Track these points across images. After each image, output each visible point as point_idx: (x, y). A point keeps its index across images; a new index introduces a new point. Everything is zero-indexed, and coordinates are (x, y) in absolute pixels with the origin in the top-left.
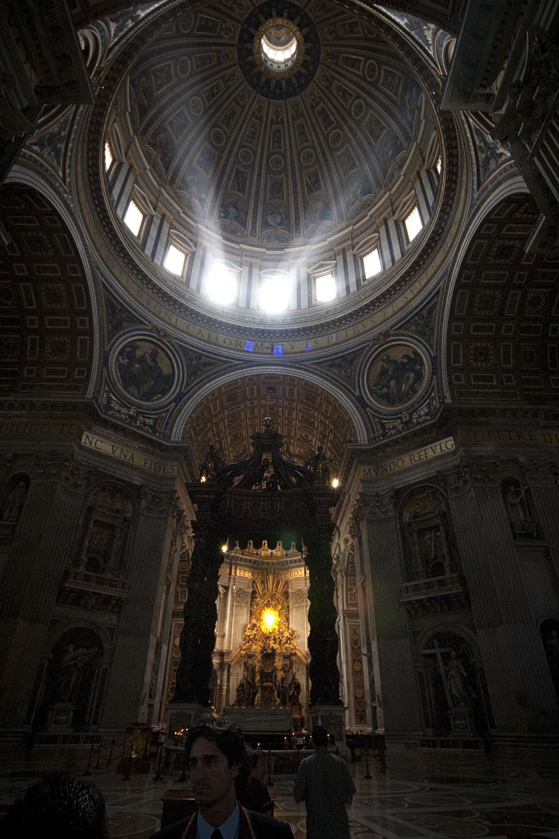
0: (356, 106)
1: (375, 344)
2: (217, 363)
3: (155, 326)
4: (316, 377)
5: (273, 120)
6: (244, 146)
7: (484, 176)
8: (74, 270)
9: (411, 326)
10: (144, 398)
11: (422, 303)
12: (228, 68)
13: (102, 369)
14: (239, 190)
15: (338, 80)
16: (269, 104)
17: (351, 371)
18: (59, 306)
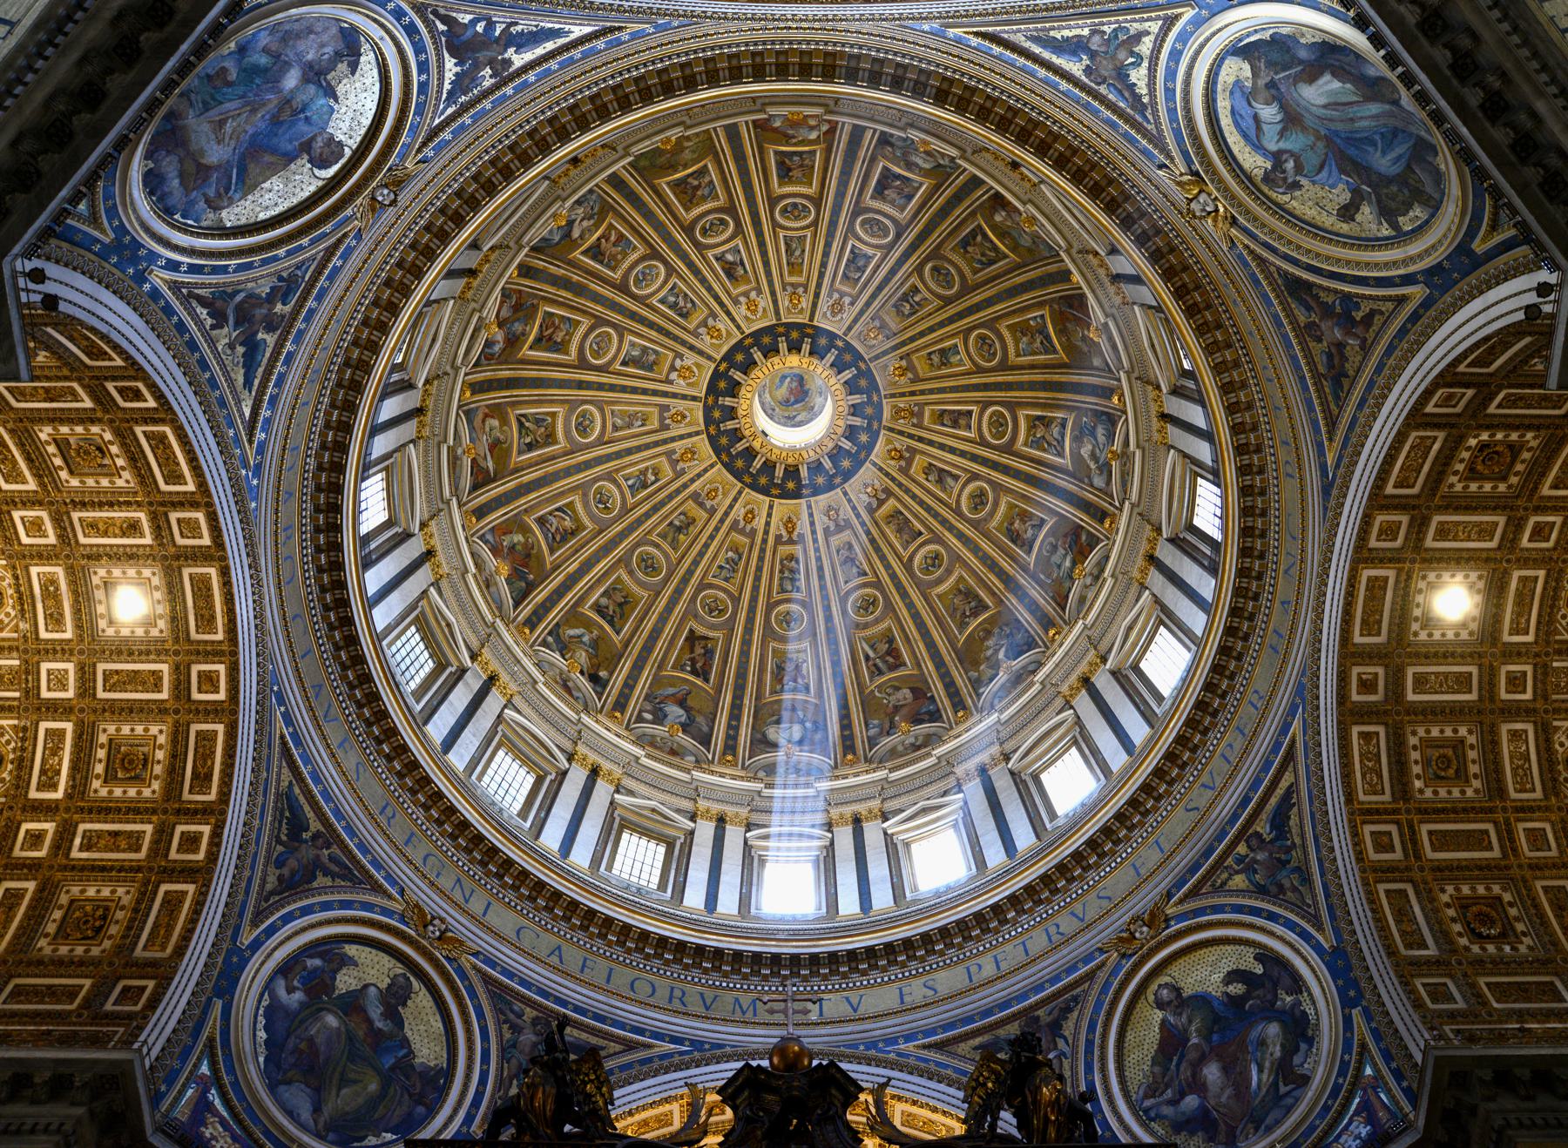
0: (972, 496)
1: (1123, 956)
2: (603, 1048)
3: (417, 906)
4: (942, 1087)
5: (778, 538)
6: (711, 586)
7: (1337, 398)
8: (209, 681)
9: (1229, 878)
10: (331, 1136)
11: (1245, 801)
12: (682, 437)
13: (210, 1000)
14: (694, 672)
15: (923, 453)
16: (771, 507)
17: (1058, 1057)
18: (132, 792)
